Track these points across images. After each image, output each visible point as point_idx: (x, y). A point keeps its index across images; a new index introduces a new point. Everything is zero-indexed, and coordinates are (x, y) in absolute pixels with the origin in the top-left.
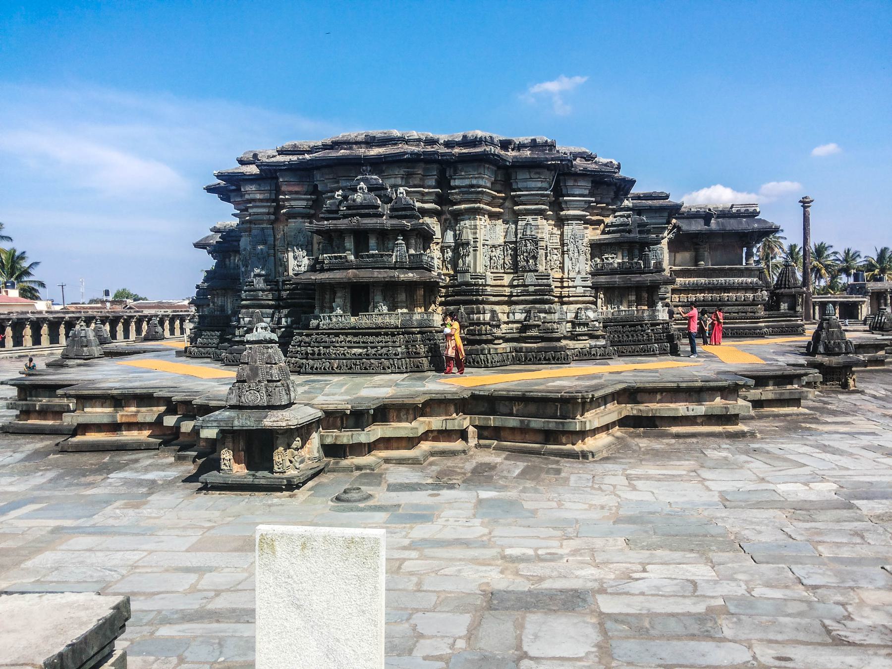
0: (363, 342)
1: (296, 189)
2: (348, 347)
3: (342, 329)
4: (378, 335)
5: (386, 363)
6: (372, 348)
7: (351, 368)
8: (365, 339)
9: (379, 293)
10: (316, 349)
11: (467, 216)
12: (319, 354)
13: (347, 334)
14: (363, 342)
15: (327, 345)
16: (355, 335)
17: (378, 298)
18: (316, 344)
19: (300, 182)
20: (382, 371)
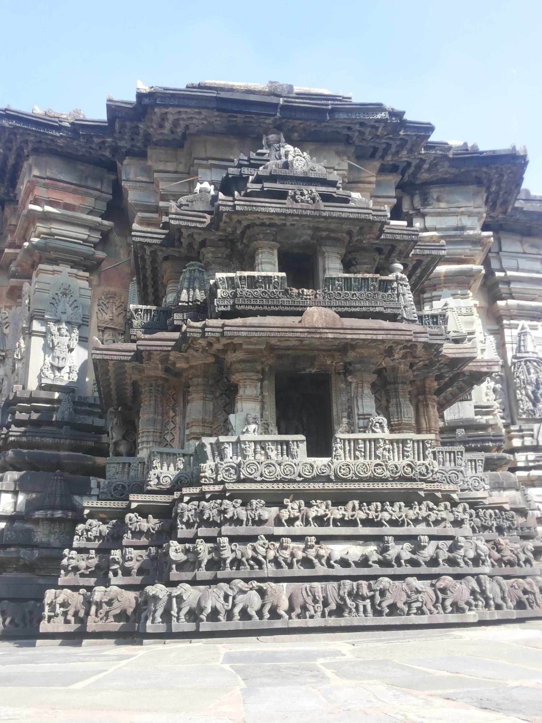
0: (367, 522)
1: (69, 199)
2: (320, 539)
3: (283, 481)
4: (410, 498)
5: (462, 591)
6: (399, 539)
7: (339, 611)
8: (372, 511)
9: (367, 391)
10: (203, 547)
11: (445, 291)
12: (216, 564)
13: (308, 497)
14: (367, 522)
15: (241, 530)
16: (339, 499)
17: (367, 404)
18: (203, 531)
19: (78, 188)
20: (453, 618)
